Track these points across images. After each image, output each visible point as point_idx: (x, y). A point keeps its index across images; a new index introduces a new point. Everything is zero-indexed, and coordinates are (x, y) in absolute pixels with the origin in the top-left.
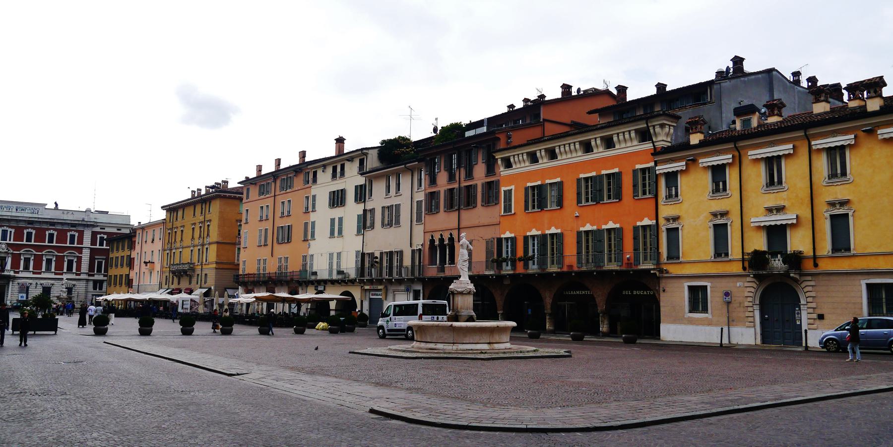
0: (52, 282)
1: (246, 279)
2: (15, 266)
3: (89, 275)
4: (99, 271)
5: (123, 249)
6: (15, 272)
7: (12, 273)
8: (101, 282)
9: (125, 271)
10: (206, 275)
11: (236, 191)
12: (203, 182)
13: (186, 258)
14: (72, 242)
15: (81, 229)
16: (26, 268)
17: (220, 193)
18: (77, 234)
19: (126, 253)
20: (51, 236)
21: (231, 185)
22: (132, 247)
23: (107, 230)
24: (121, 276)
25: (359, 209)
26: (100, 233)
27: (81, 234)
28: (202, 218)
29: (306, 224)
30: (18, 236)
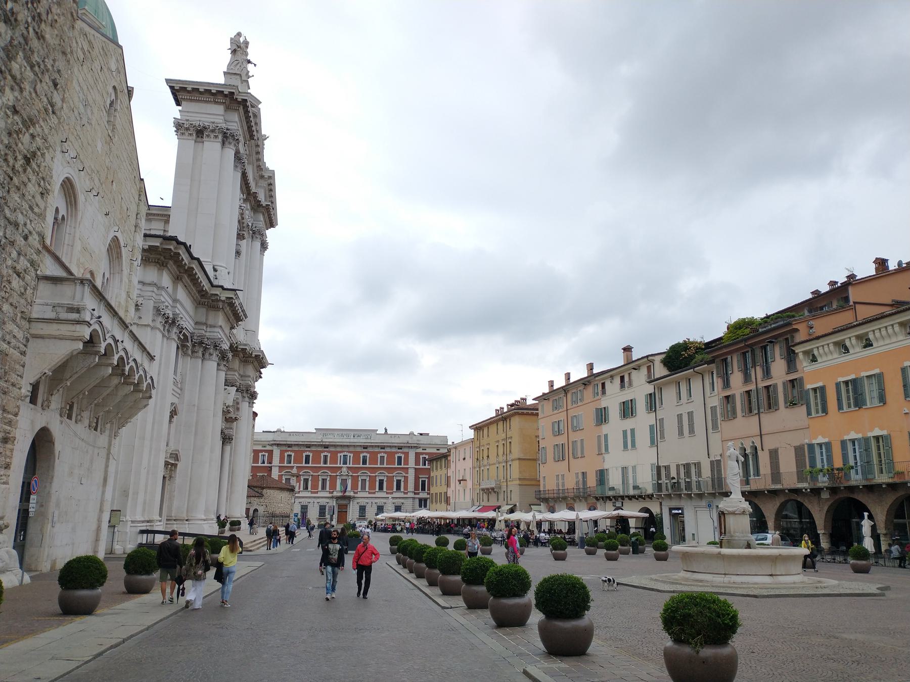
2: (354, 487)
4: (423, 489)
5: (441, 468)
6: (355, 493)
7: (352, 494)
8: (426, 500)
9: (443, 489)
11: (534, 408)
12: (504, 402)
14: (399, 463)
15: (406, 450)
16: (363, 488)
17: (519, 409)
18: (403, 456)
20: (382, 458)
21: (530, 402)
22: (447, 466)
23: (428, 451)
24: (441, 493)
25: (651, 419)
26: (423, 454)
27: (407, 454)
28: (504, 436)
29: (599, 437)
30: (356, 461)
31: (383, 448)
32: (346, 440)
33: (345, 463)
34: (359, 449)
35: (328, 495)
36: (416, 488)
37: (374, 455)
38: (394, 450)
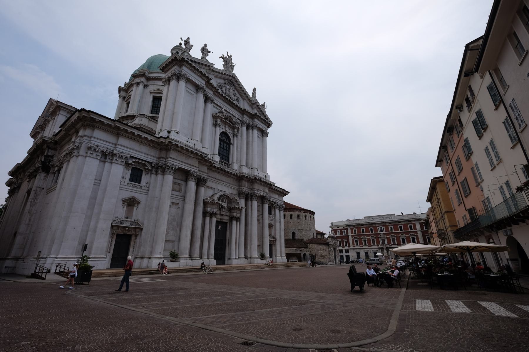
2: (389, 242)
29: (472, 169)
30: (387, 229)
31: (400, 222)
32: (379, 221)
34: (387, 224)
35: (376, 247)
37: (406, 226)
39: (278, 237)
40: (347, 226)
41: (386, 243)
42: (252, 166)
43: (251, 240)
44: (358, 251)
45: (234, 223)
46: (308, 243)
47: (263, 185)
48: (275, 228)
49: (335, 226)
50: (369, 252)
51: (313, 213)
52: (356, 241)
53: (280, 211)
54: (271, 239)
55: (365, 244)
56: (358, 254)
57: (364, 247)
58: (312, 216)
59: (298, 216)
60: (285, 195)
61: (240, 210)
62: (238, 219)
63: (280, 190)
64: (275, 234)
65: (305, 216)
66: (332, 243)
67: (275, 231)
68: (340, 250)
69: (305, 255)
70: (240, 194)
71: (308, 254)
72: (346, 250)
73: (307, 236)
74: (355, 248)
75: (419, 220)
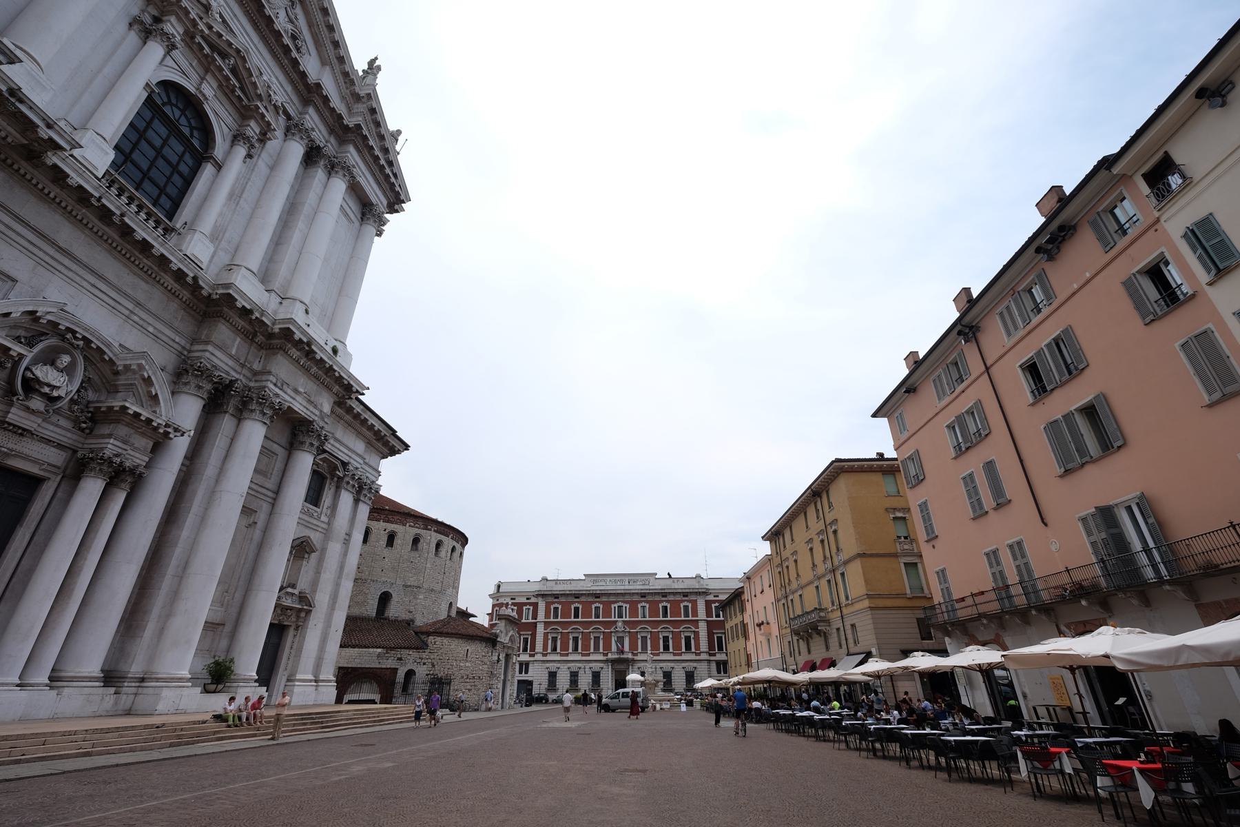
0: (672, 665)
1: (962, 614)
2: (633, 647)
3: (710, 655)
7: (630, 656)
10: (853, 626)
13: (811, 603)
14: (687, 615)
15: (693, 598)
19: (739, 618)
22: (743, 610)
26: (714, 602)
27: (694, 603)
28: (821, 526)
30: (634, 612)
31: (664, 595)
32: (619, 587)
33: (620, 616)
34: (636, 598)
35: (601, 658)
36: (711, 646)
38: (678, 598)
39: (321, 599)
40: (537, 596)
41: (627, 648)
42: (288, 284)
43: (175, 595)
44: (553, 667)
45: (92, 488)
46: (428, 634)
47: (317, 378)
48: (321, 561)
49: (506, 594)
50: (581, 672)
51: (463, 539)
52: (555, 640)
53: (357, 501)
54: (288, 602)
55: (576, 649)
56: (553, 676)
57: (570, 658)
58: (458, 546)
59: (416, 541)
60: (393, 452)
61: (159, 440)
62: (126, 480)
63: (378, 426)
64: (315, 584)
65: (439, 545)
66: (504, 639)
67: (318, 572)
68: (521, 664)
69: (410, 674)
70: (185, 371)
71: (422, 672)
72: (521, 664)
73: (426, 613)
74: (549, 658)
75: (706, 593)
